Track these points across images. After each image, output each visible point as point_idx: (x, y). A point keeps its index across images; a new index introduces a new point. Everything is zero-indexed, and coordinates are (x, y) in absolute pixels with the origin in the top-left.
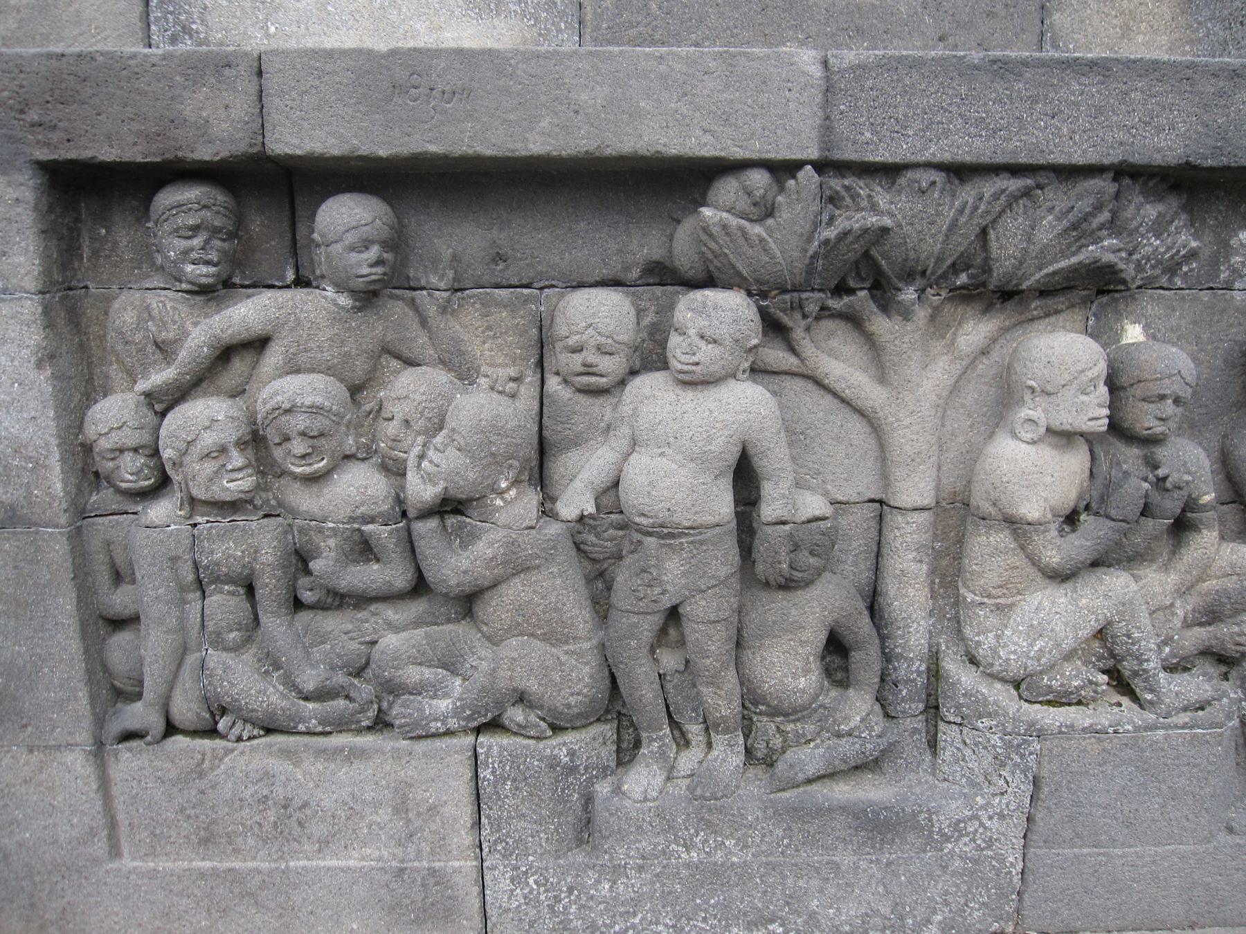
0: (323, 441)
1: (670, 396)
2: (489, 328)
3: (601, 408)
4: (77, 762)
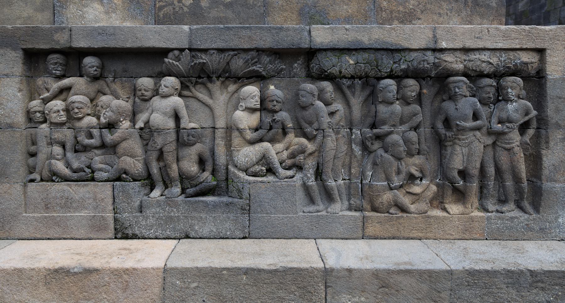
0: (82, 110)
1: (159, 100)
2: (123, 87)
3: (144, 104)
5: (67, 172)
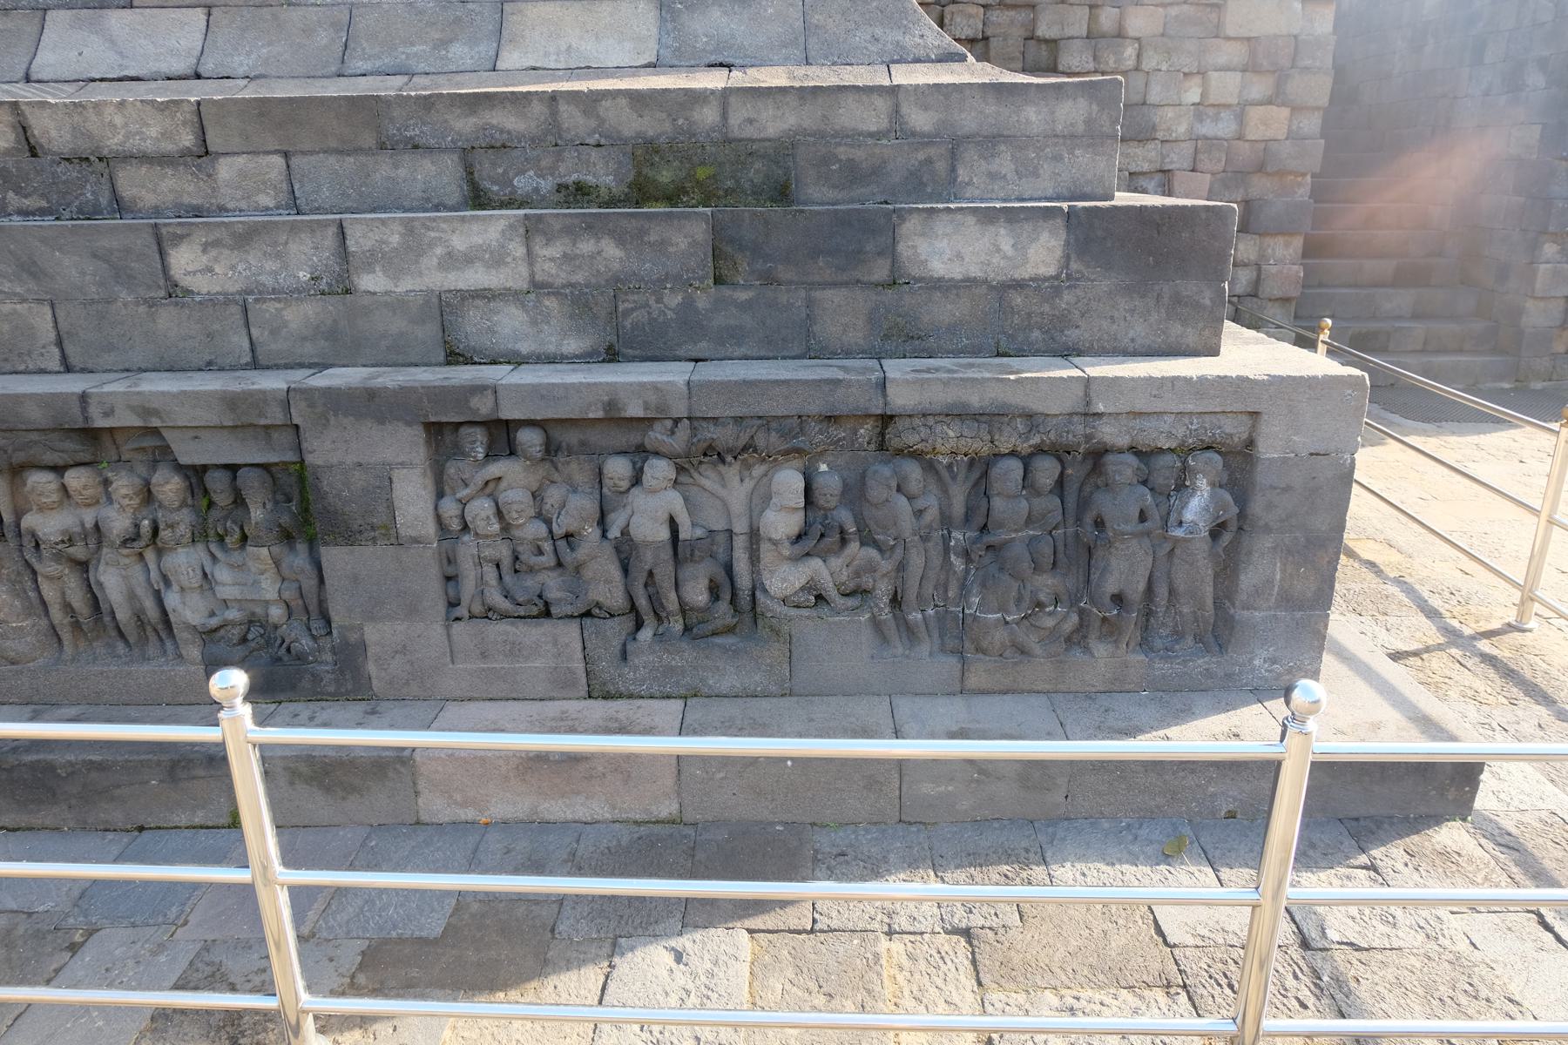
4: (438, 630)
5: (505, 605)
